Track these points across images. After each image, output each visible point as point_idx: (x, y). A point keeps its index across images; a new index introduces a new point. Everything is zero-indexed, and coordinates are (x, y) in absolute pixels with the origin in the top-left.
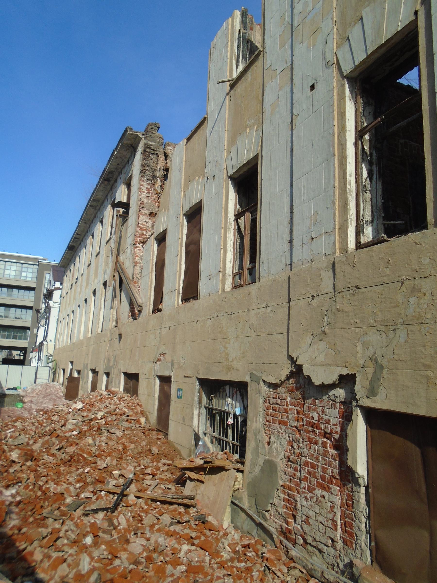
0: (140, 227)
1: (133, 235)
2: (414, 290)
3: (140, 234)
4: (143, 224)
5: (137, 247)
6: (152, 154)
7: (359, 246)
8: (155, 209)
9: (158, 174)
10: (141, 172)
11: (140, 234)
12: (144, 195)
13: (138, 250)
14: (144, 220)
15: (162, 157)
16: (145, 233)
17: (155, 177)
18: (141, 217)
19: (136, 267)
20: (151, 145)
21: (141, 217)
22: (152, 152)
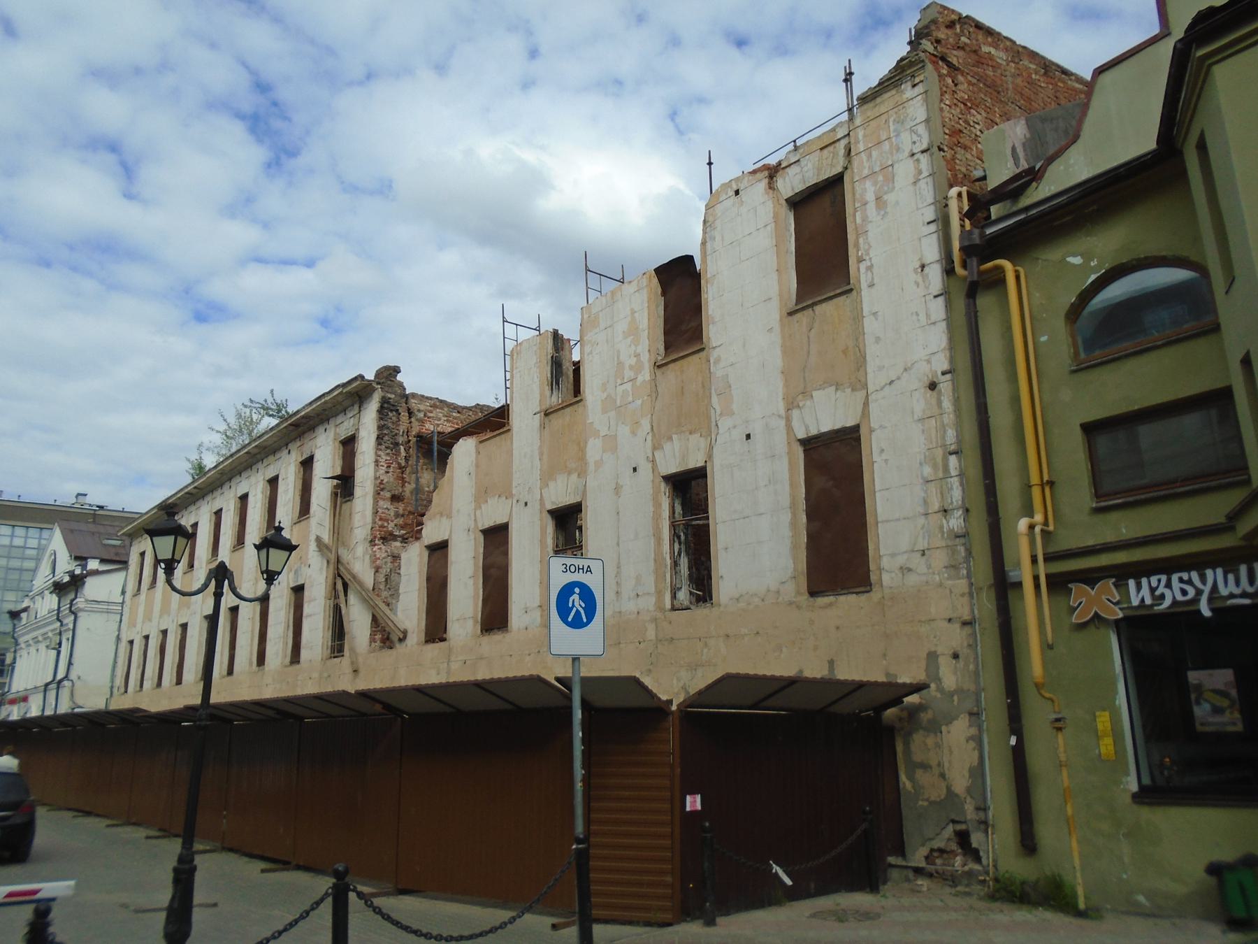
2: (706, 645)
7: (673, 609)
9: (401, 440)
10: (379, 439)
15: (404, 415)
17: (397, 444)
21: (381, 503)
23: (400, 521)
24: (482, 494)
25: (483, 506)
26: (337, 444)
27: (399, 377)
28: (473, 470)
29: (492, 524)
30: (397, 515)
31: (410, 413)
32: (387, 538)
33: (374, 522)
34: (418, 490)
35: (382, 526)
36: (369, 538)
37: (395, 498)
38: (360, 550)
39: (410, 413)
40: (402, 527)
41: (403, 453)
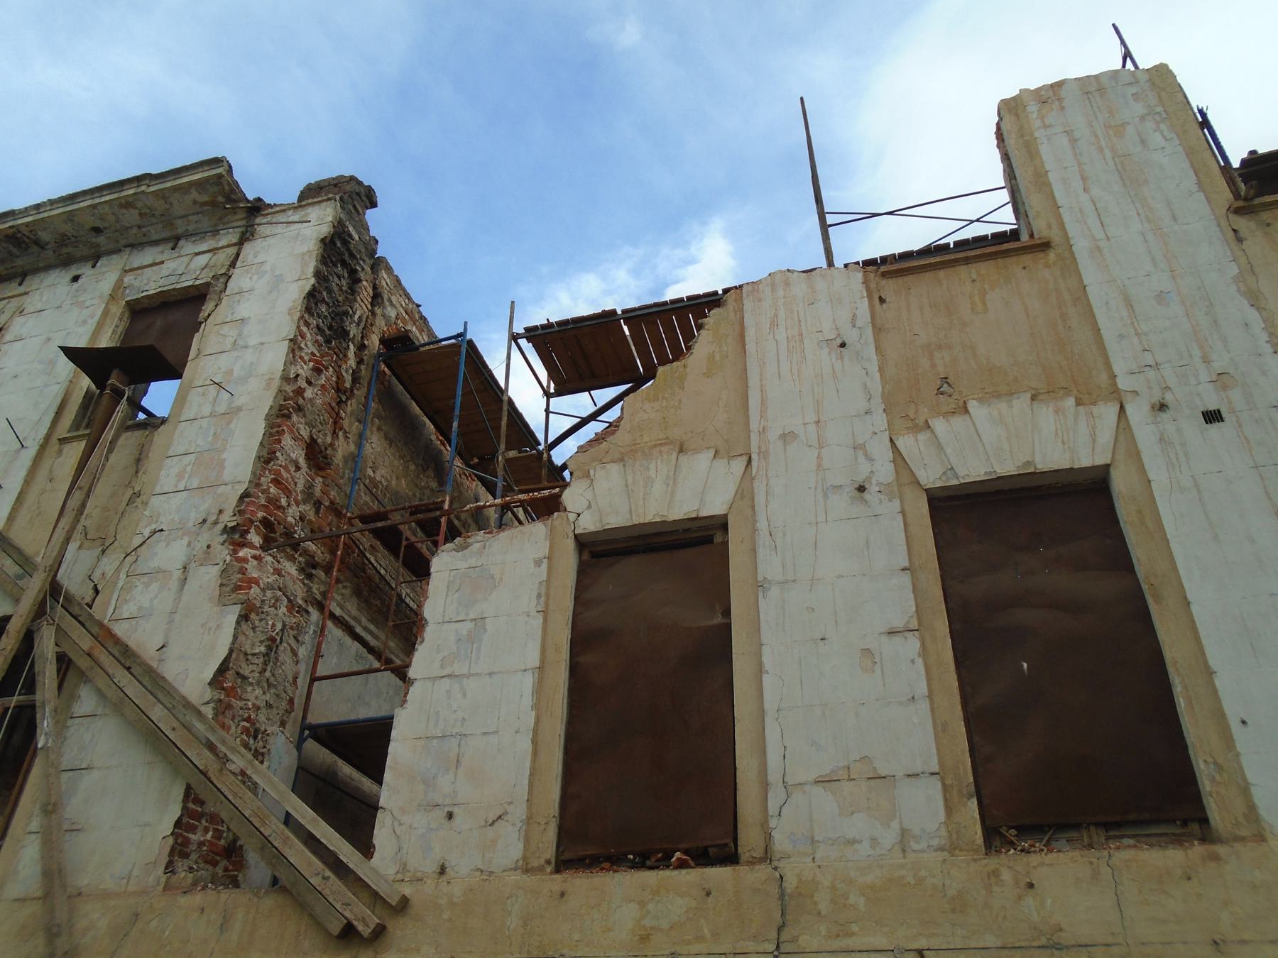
0: (278, 473)
1: (241, 490)
3: (269, 500)
4: (285, 467)
5: (245, 544)
6: (344, 264)
8: (325, 435)
9: (353, 331)
11: (269, 500)
12: (304, 370)
13: (254, 557)
14: (293, 456)
16: (284, 502)
18: (287, 441)
19: (244, 626)
20: (350, 236)
22: (346, 257)
23: (308, 509)
24: (922, 393)
25: (939, 425)
26: (118, 309)
27: (370, 215)
28: (862, 339)
29: (1007, 466)
30: (308, 493)
31: (377, 297)
32: (277, 537)
33: (255, 482)
34: (354, 459)
35: (273, 502)
36: (228, 519)
37: (317, 456)
38: (169, 554)
39: (377, 297)
40: (314, 533)
41: (352, 362)
